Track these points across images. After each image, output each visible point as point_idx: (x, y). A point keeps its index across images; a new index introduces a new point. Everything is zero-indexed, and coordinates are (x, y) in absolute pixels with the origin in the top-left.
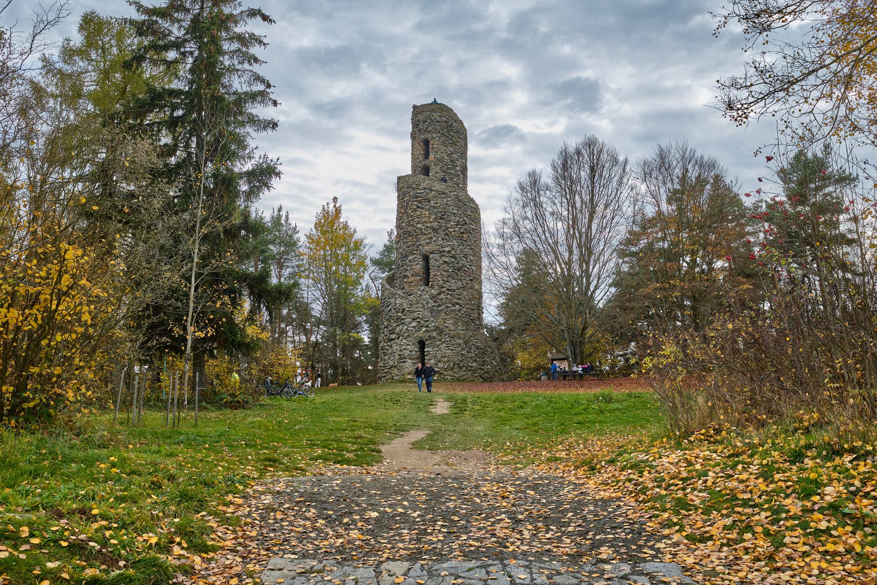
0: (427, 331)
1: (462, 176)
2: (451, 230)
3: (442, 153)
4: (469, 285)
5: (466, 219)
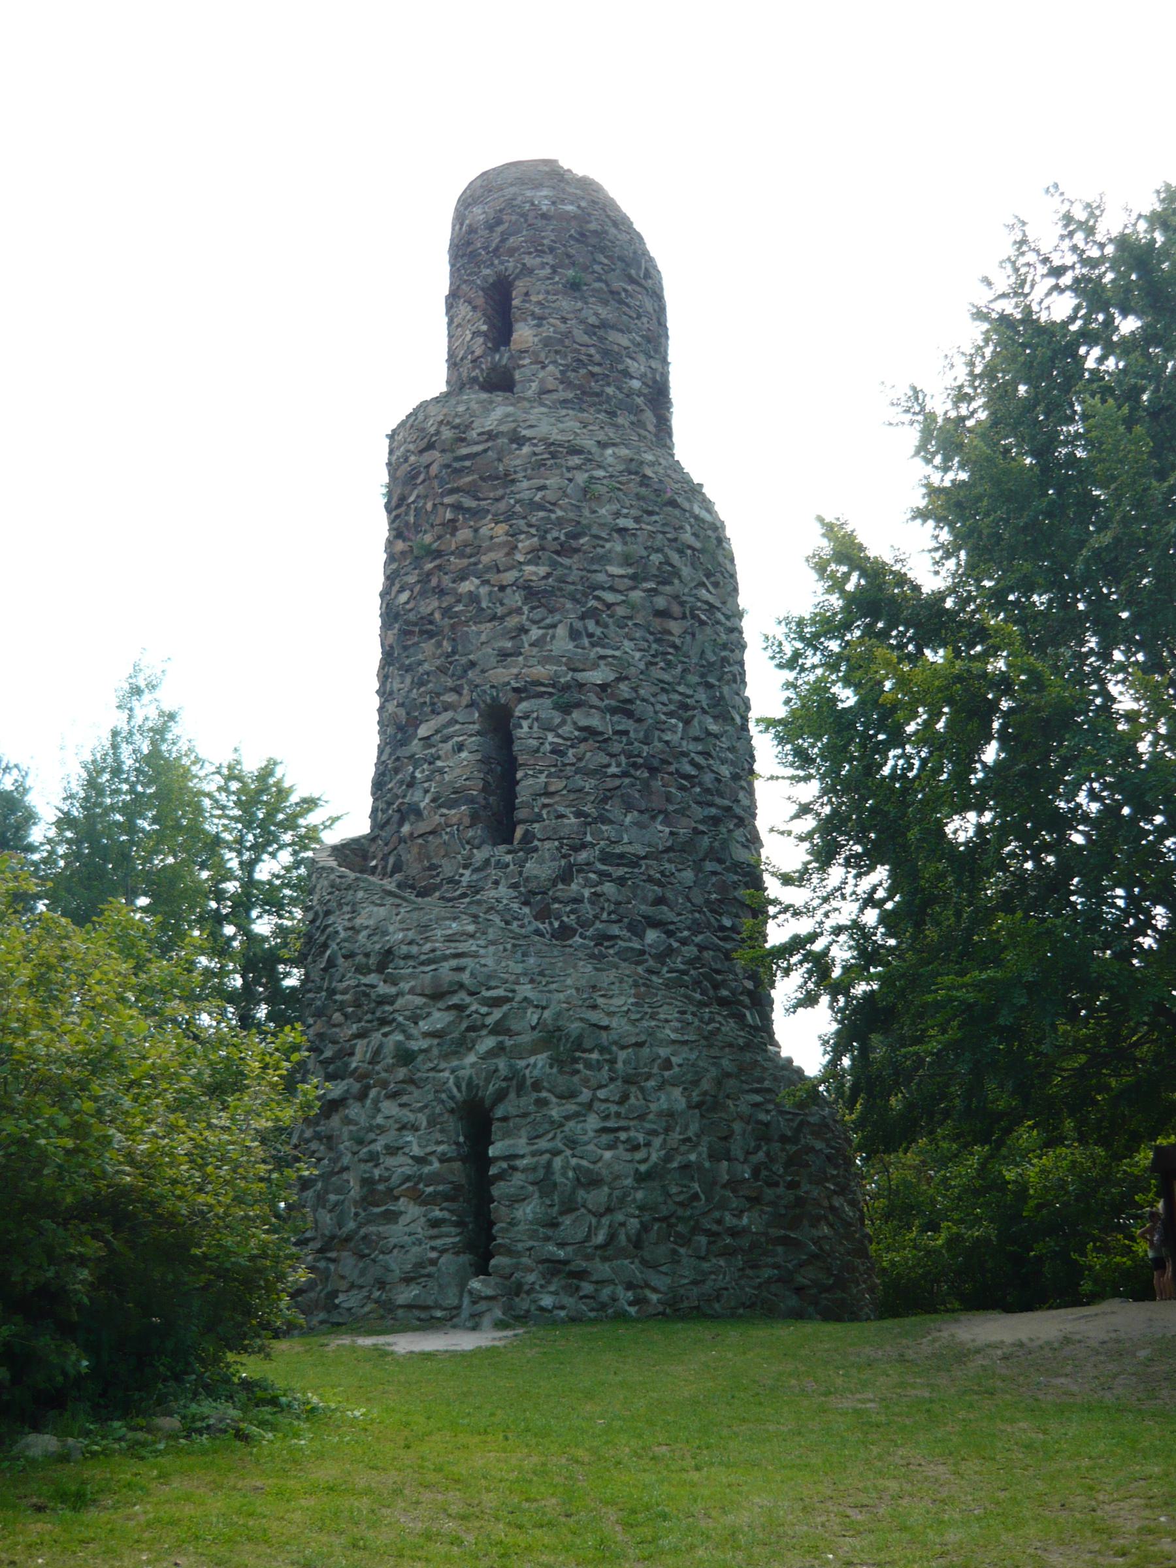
0: (500, 1049)
1: (649, 417)
2: (610, 597)
3: (564, 320)
4: (706, 841)
5: (675, 558)
